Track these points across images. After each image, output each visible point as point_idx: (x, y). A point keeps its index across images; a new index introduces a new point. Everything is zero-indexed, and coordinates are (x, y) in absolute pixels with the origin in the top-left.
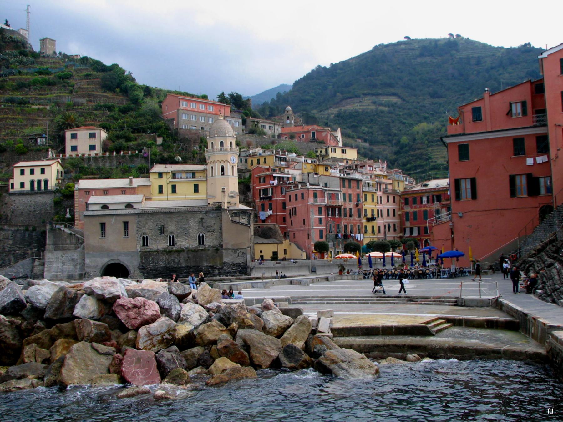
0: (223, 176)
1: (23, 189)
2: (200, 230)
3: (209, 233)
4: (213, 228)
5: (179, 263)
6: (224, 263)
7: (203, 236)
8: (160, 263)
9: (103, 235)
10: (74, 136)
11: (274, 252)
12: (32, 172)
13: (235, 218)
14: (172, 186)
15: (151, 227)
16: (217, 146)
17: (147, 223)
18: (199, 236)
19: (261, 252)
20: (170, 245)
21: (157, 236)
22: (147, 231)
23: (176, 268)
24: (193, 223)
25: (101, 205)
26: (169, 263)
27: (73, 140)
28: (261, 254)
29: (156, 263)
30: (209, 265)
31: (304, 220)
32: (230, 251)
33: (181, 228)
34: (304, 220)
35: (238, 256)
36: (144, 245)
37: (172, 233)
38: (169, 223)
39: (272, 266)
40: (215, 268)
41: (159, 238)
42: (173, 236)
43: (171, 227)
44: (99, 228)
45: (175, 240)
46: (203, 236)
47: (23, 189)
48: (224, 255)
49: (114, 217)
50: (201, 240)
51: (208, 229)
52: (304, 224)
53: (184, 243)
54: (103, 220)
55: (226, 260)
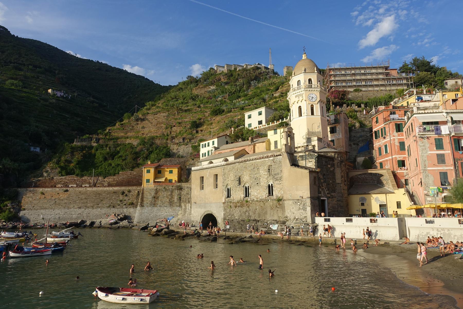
0: (301, 117)
2: (269, 179)
3: (276, 182)
4: (280, 176)
7: (272, 184)
9: (202, 188)
10: (250, 117)
12: (208, 146)
13: (301, 161)
15: (232, 179)
16: (295, 85)
17: (229, 174)
18: (269, 184)
20: (246, 196)
21: (237, 188)
22: (229, 182)
24: (263, 172)
25: (208, 162)
26: (241, 215)
28: (363, 208)
31: (416, 159)
32: (291, 202)
34: (416, 159)
35: (300, 209)
36: (228, 197)
41: (238, 189)
42: (248, 186)
43: (246, 178)
44: (199, 181)
45: (250, 191)
46: (272, 184)
49: (209, 170)
50: (270, 189)
51: (276, 177)
52: (417, 166)
54: (202, 173)
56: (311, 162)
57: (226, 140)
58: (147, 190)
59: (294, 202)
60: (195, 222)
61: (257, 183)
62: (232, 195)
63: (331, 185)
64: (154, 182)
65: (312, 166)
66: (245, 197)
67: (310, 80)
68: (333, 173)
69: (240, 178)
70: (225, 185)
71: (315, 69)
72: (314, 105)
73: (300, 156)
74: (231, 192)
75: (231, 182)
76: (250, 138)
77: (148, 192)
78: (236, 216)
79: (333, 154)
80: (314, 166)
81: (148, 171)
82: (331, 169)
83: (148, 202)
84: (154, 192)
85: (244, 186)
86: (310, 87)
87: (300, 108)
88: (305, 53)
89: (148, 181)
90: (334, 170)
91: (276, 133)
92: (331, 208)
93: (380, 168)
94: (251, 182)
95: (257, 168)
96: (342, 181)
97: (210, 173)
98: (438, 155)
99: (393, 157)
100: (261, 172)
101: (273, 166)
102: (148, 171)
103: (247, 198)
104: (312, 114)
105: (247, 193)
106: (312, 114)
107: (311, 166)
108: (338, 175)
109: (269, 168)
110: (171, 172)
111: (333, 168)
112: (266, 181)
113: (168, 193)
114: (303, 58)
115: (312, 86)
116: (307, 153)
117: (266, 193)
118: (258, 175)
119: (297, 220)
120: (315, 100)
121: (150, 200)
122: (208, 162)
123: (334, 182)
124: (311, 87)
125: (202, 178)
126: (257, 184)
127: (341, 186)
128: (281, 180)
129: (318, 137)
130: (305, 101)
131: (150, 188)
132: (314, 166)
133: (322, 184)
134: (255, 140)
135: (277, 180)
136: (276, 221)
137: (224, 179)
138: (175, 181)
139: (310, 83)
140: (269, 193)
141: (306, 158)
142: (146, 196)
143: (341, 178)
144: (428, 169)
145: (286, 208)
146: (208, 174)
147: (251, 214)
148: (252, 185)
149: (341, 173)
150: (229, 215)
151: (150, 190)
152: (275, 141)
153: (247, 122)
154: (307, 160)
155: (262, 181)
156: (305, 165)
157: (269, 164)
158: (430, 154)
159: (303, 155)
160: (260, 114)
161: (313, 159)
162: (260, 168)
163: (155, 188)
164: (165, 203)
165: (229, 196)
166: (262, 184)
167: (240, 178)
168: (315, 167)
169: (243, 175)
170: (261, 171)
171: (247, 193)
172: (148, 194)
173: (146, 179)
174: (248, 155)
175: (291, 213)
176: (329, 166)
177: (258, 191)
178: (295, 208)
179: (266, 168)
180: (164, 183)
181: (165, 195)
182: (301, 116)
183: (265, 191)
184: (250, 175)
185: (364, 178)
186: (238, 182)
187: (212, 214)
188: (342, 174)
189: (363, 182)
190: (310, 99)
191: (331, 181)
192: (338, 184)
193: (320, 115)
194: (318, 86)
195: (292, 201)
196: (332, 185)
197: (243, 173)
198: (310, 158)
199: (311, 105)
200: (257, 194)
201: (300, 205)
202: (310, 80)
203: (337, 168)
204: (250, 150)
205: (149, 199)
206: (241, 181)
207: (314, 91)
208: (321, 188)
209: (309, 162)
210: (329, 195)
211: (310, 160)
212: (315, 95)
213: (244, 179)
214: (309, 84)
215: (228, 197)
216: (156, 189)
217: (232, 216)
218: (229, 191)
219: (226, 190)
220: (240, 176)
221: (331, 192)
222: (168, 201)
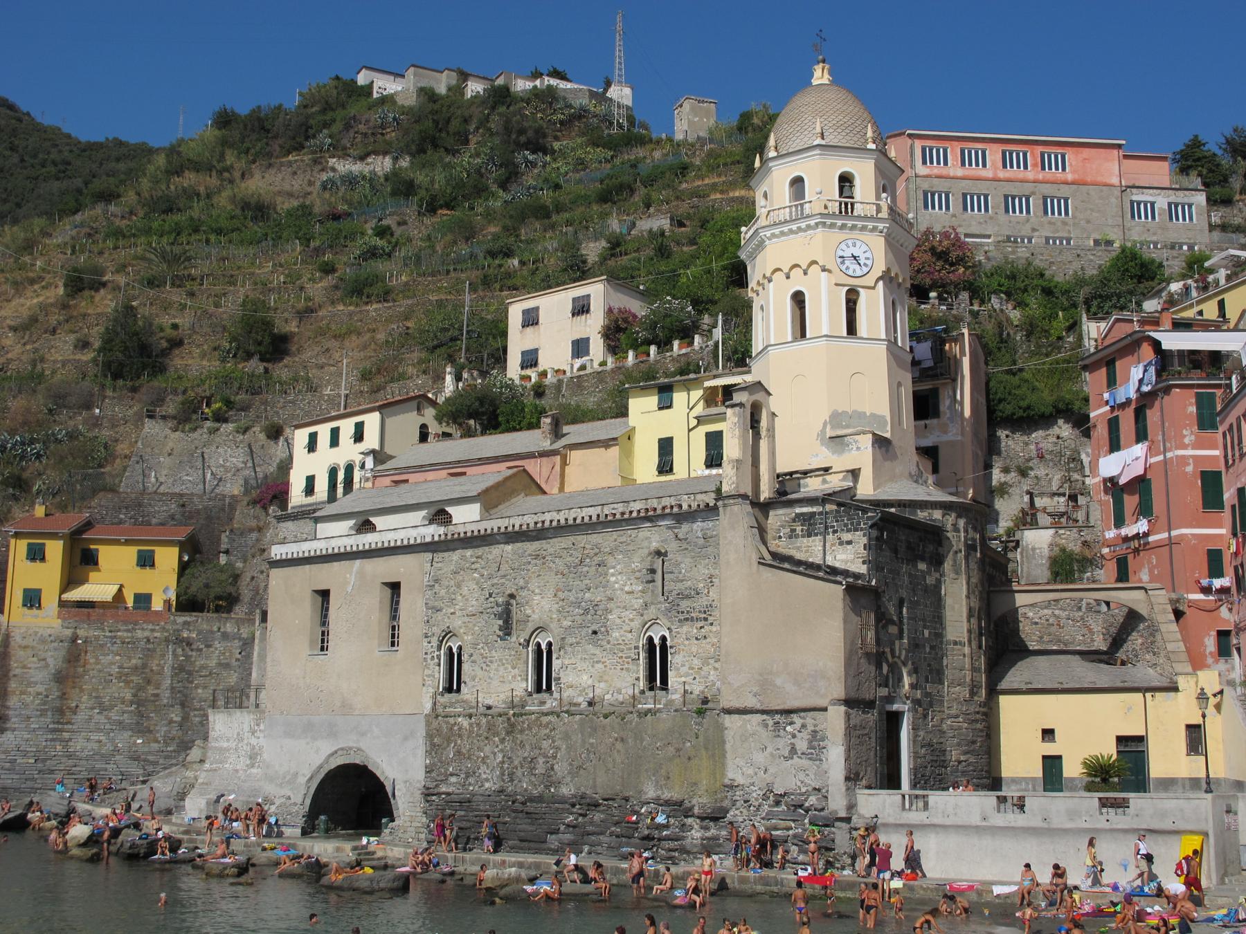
0: (803, 344)
1: (310, 500)
2: (652, 612)
3: (685, 629)
4: (703, 601)
5: (549, 779)
6: (731, 787)
7: (663, 639)
8: (484, 772)
10: (531, 319)
11: (1121, 740)
12: (335, 441)
13: (805, 540)
14: (708, 435)
15: (474, 605)
17: (459, 586)
18: (650, 639)
19: (1048, 734)
20: (539, 689)
22: (457, 623)
23: (540, 799)
27: (529, 330)
28: (1051, 749)
29: (468, 775)
30: (666, 795)
33: (577, 604)
35: (793, 750)
36: (449, 689)
37: (540, 629)
38: (533, 585)
39: (976, 820)
40: (688, 813)
42: (550, 644)
44: (306, 610)
45: (556, 664)
46: (663, 639)
47: (310, 500)
48: (729, 735)
49: (358, 562)
51: (684, 604)
53: (585, 680)
55: (736, 772)
56: (849, 547)
57: (421, 420)
58: (24, 643)
59: (771, 723)
60: (278, 802)
61: (595, 627)
62: (470, 684)
63: (928, 649)
64: (63, 604)
65: (852, 562)
66: (530, 694)
67: (846, 180)
68: (935, 596)
69: (508, 604)
70: (437, 630)
71: (870, 134)
72: (860, 289)
73: (802, 514)
74: (465, 667)
75: (467, 619)
76: (546, 421)
77: (30, 652)
78: (487, 780)
79: (937, 514)
80: (864, 562)
81: (36, 554)
82: (930, 580)
83: (29, 699)
84: (63, 652)
85: (528, 642)
86: (846, 212)
87: (799, 299)
88: (824, 61)
89: (32, 599)
90: (939, 582)
91: (666, 405)
92: (923, 751)
93: (1119, 580)
94: (566, 623)
95: (597, 559)
96: (970, 631)
97: (361, 574)
99: (1174, 533)
100: (613, 579)
101: (670, 556)
102: (36, 554)
103: (545, 695)
104: (852, 329)
105: (543, 680)
106: (852, 329)
107: (846, 561)
109: (652, 563)
110: (146, 561)
111: (937, 575)
112: (636, 624)
113: (130, 658)
114: (815, 82)
116: (829, 507)
117: (635, 675)
118: (597, 596)
119: (777, 803)
120: (865, 270)
121: (40, 688)
122: (351, 523)
124: (847, 208)
125: (325, 594)
126: (595, 633)
127: (964, 655)
128: (706, 619)
129: (874, 434)
130: (824, 270)
131: (41, 632)
132: (864, 562)
133: (894, 644)
134: (566, 429)
135: (687, 619)
136: (681, 803)
137: (431, 603)
138: (167, 603)
139: (846, 189)
140: (651, 678)
141: (826, 528)
142: (18, 671)
143: (969, 621)
145: (728, 746)
146: (352, 579)
147: (561, 768)
148: (571, 640)
149: (968, 597)
150: (452, 775)
151: (43, 641)
152: (660, 441)
153: (518, 341)
154: (830, 537)
155: (618, 621)
156: (820, 555)
157: (655, 545)
159: (813, 514)
160: (581, 308)
161: (856, 530)
162: (610, 561)
163: (68, 632)
164: (112, 707)
165: (452, 685)
166: (616, 634)
167: (508, 604)
168: (863, 569)
169: (524, 593)
170: (613, 575)
171: (543, 680)
172: (33, 662)
173: (25, 591)
174: (541, 497)
175: (750, 771)
177: (600, 666)
178: (769, 750)
179: (639, 562)
180: (110, 612)
181: (114, 669)
182: (803, 335)
183: (628, 670)
184: (560, 594)
185: (1051, 621)
186: (501, 622)
187: (365, 767)
189: (1046, 638)
191: (926, 633)
192: (955, 643)
193: (883, 336)
194: (879, 210)
195: (759, 717)
196: (932, 648)
197: (527, 583)
198: (846, 525)
199: (848, 292)
200: (590, 682)
201: (794, 736)
202: (846, 180)
203: (953, 575)
204: (545, 472)
205: (36, 683)
206: (516, 614)
208: (887, 662)
209: (841, 543)
210: (918, 694)
211: (847, 536)
212: (866, 248)
213: (529, 612)
214: (841, 194)
215: (449, 689)
216: (74, 639)
217: (468, 775)
218: (454, 663)
219: (439, 657)
220: (512, 596)
221: (927, 678)
222: (128, 696)
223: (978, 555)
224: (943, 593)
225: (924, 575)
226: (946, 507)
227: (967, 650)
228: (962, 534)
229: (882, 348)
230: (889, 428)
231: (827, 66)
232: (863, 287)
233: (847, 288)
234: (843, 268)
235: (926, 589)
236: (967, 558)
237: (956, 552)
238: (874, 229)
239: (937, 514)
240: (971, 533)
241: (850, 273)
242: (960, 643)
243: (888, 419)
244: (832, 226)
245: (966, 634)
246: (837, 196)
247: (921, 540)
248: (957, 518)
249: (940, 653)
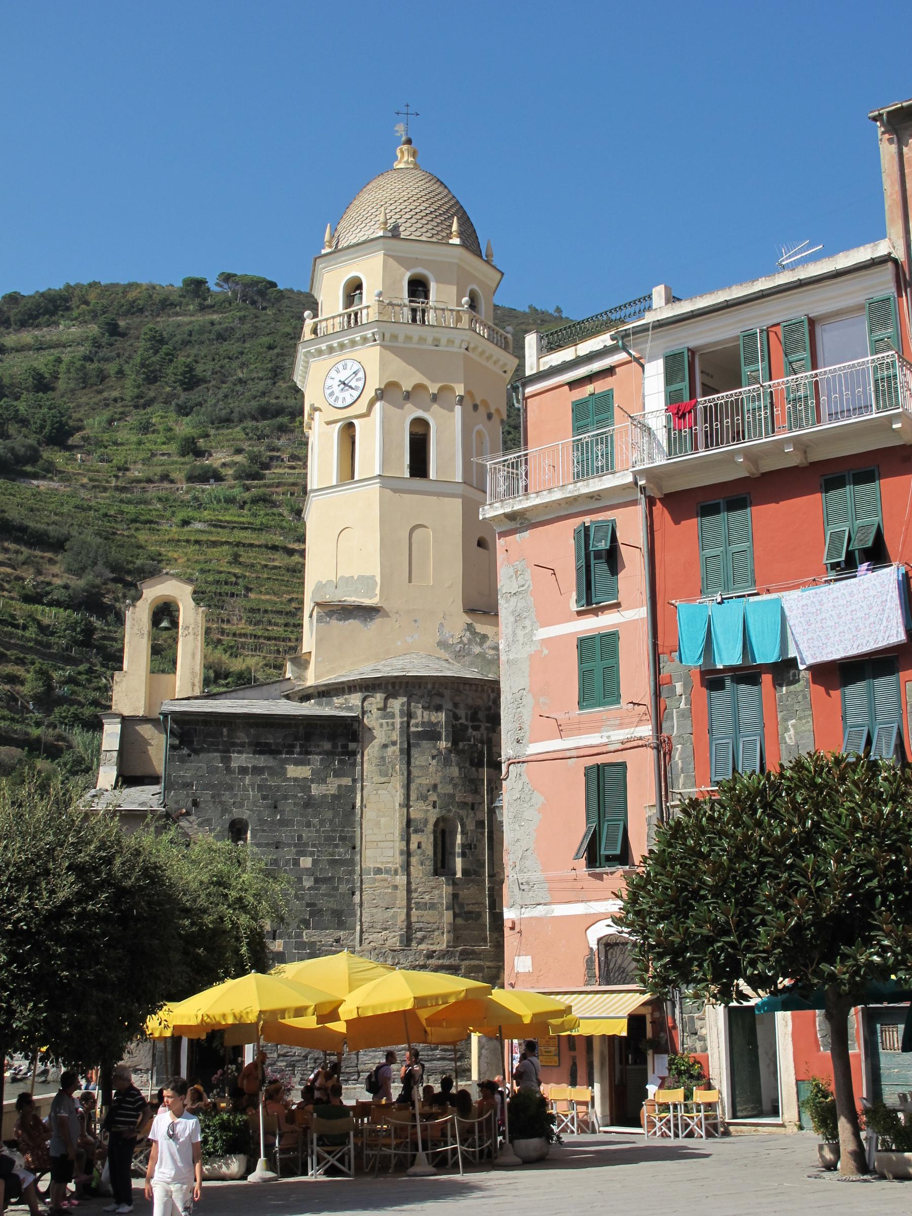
63: (308, 883)
72: (355, 421)
98: (585, 644)
108: (383, 820)
111: (347, 781)
115: (356, 314)
120: (356, 394)
123: (333, 863)
127: (396, 887)
144: (534, 749)
158: (546, 642)
176: (293, 771)
188: (422, 811)
190: (332, 394)
192: (378, 871)
203: (379, 779)
207: (353, 343)
223: (443, 744)
224: (358, 804)
225: (303, 785)
226: (368, 686)
227: (401, 880)
228: (398, 720)
229: (375, 488)
230: (378, 591)
231: (405, 147)
232: (357, 417)
233: (339, 424)
234: (331, 401)
235: (309, 803)
236: (407, 753)
237: (385, 746)
238: (365, 340)
239: (355, 699)
240: (421, 715)
241: (340, 404)
242: (387, 871)
243: (378, 579)
244: (320, 352)
245: (398, 861)
246: (341, 310)
247: (297, 738)
248: (386, 699)
249: (343, 888)
